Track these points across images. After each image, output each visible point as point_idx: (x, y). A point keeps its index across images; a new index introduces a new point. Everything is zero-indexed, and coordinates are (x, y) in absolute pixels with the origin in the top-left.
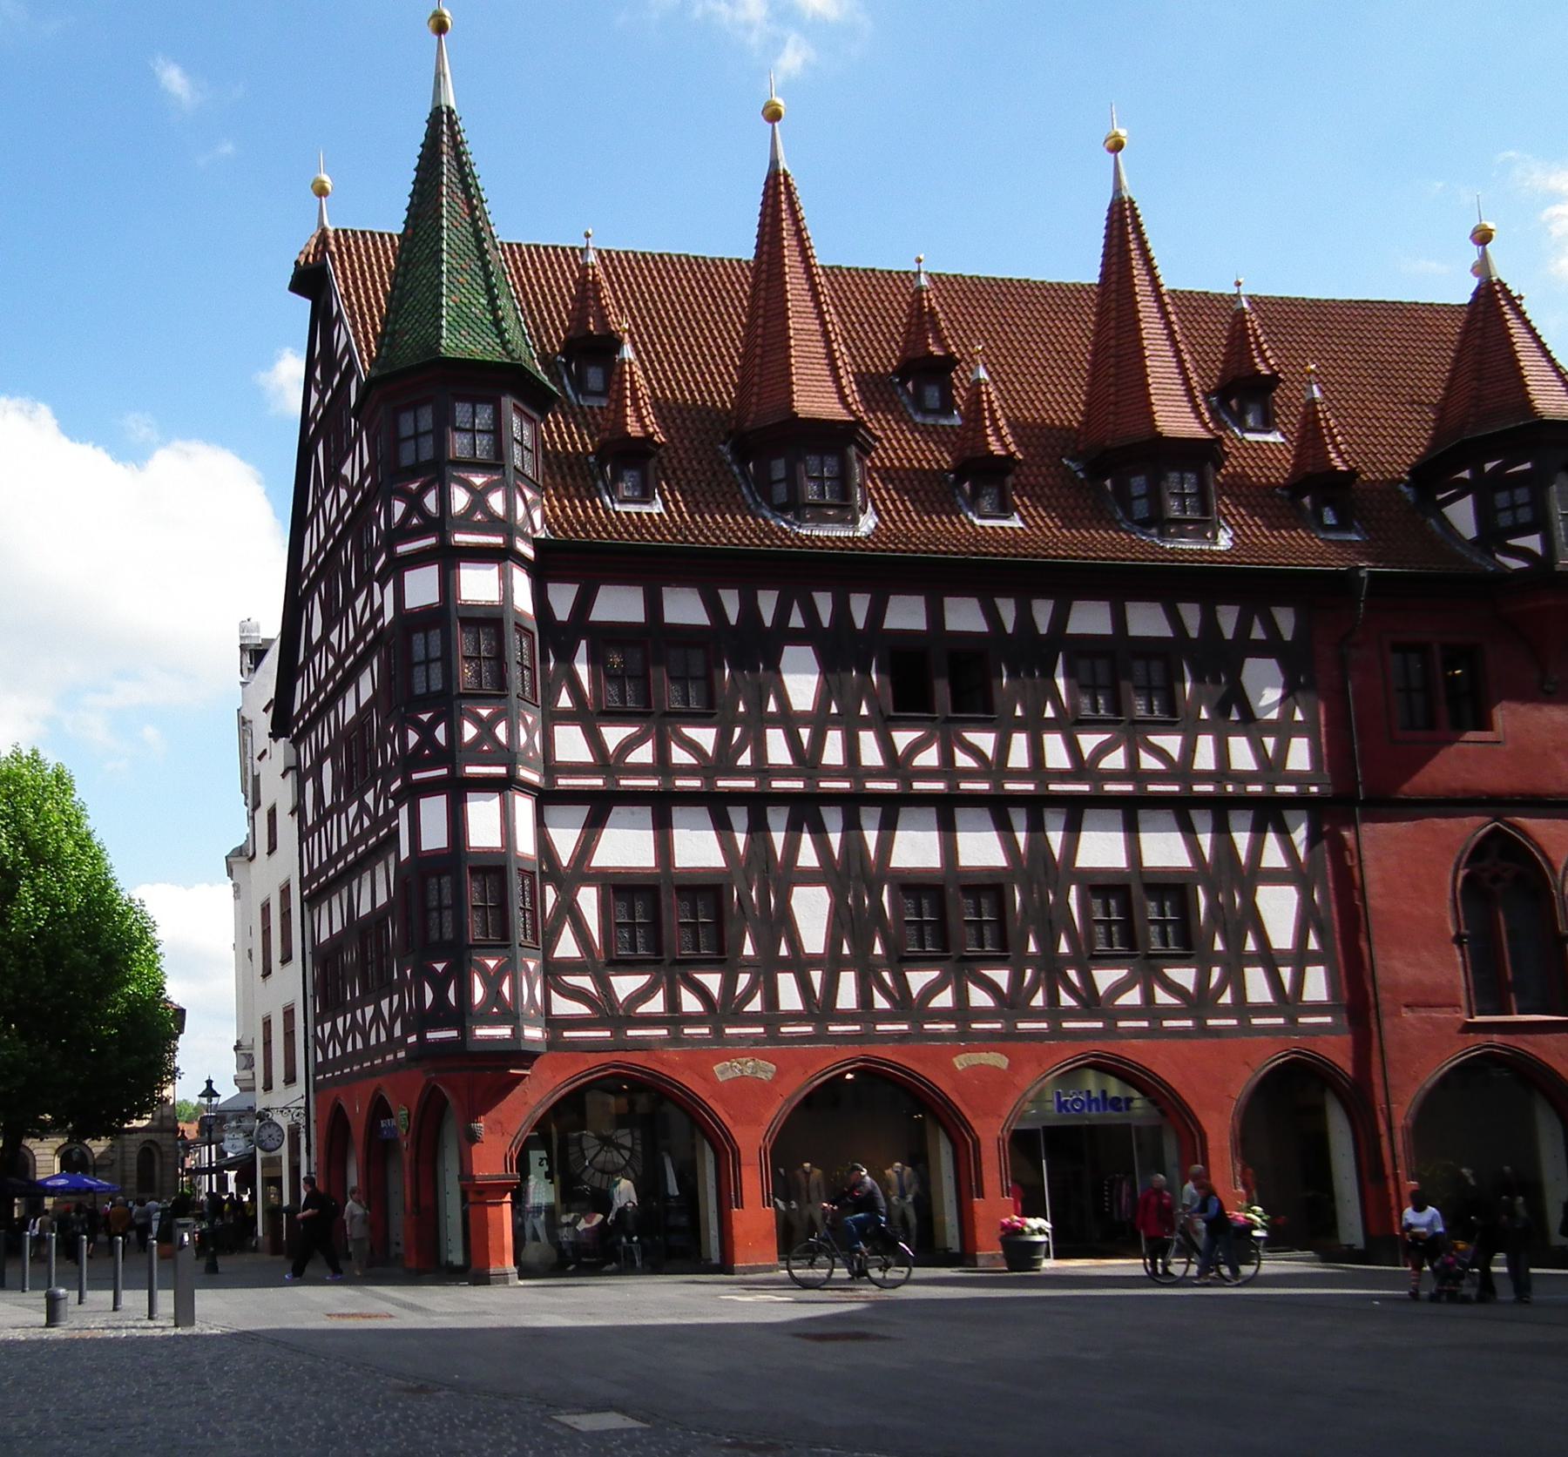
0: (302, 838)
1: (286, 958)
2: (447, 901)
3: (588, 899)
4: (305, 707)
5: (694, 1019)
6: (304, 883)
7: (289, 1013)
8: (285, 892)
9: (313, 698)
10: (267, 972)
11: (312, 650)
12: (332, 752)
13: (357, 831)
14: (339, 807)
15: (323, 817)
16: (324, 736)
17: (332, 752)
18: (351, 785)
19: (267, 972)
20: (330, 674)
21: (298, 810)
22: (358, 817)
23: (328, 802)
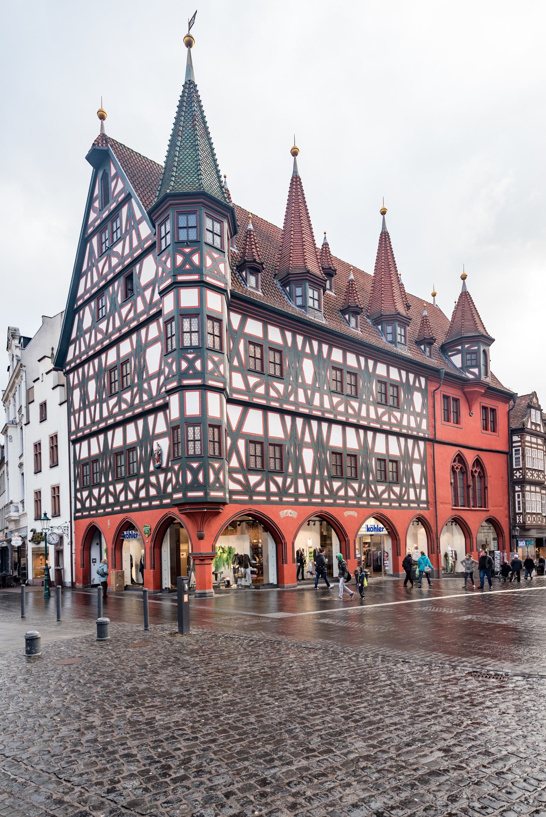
0: (71, 412)
1: (54, 464)
2: (216, 440)
3: (241, 444)
4: (75, 358)
5: (274, 494)
6: (70, 433)
7: (56, 489)
8: (54, 438)
9: (81, 354)
10: (38, 470)
11: (81, 333)
12: (98, 376)
13: (116, 410)
14: (100, 401)
15: (85, 404)
16: (90, 369)
17: (98, 376)
18: (109, 391)
19: (38, 470)
20: (97, 343)
21: (69, 401)
22: (118, 403)
23: (92, 397)
